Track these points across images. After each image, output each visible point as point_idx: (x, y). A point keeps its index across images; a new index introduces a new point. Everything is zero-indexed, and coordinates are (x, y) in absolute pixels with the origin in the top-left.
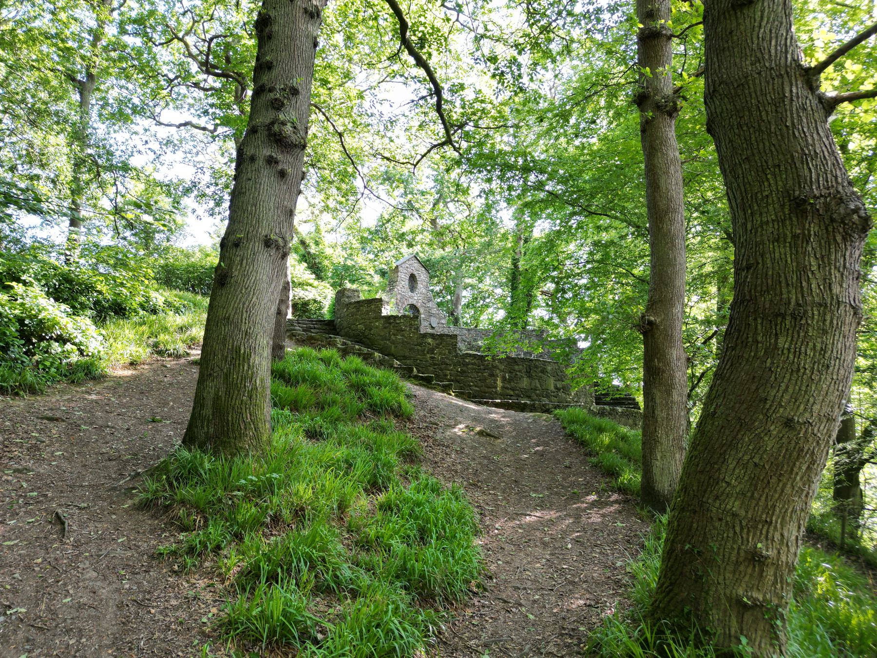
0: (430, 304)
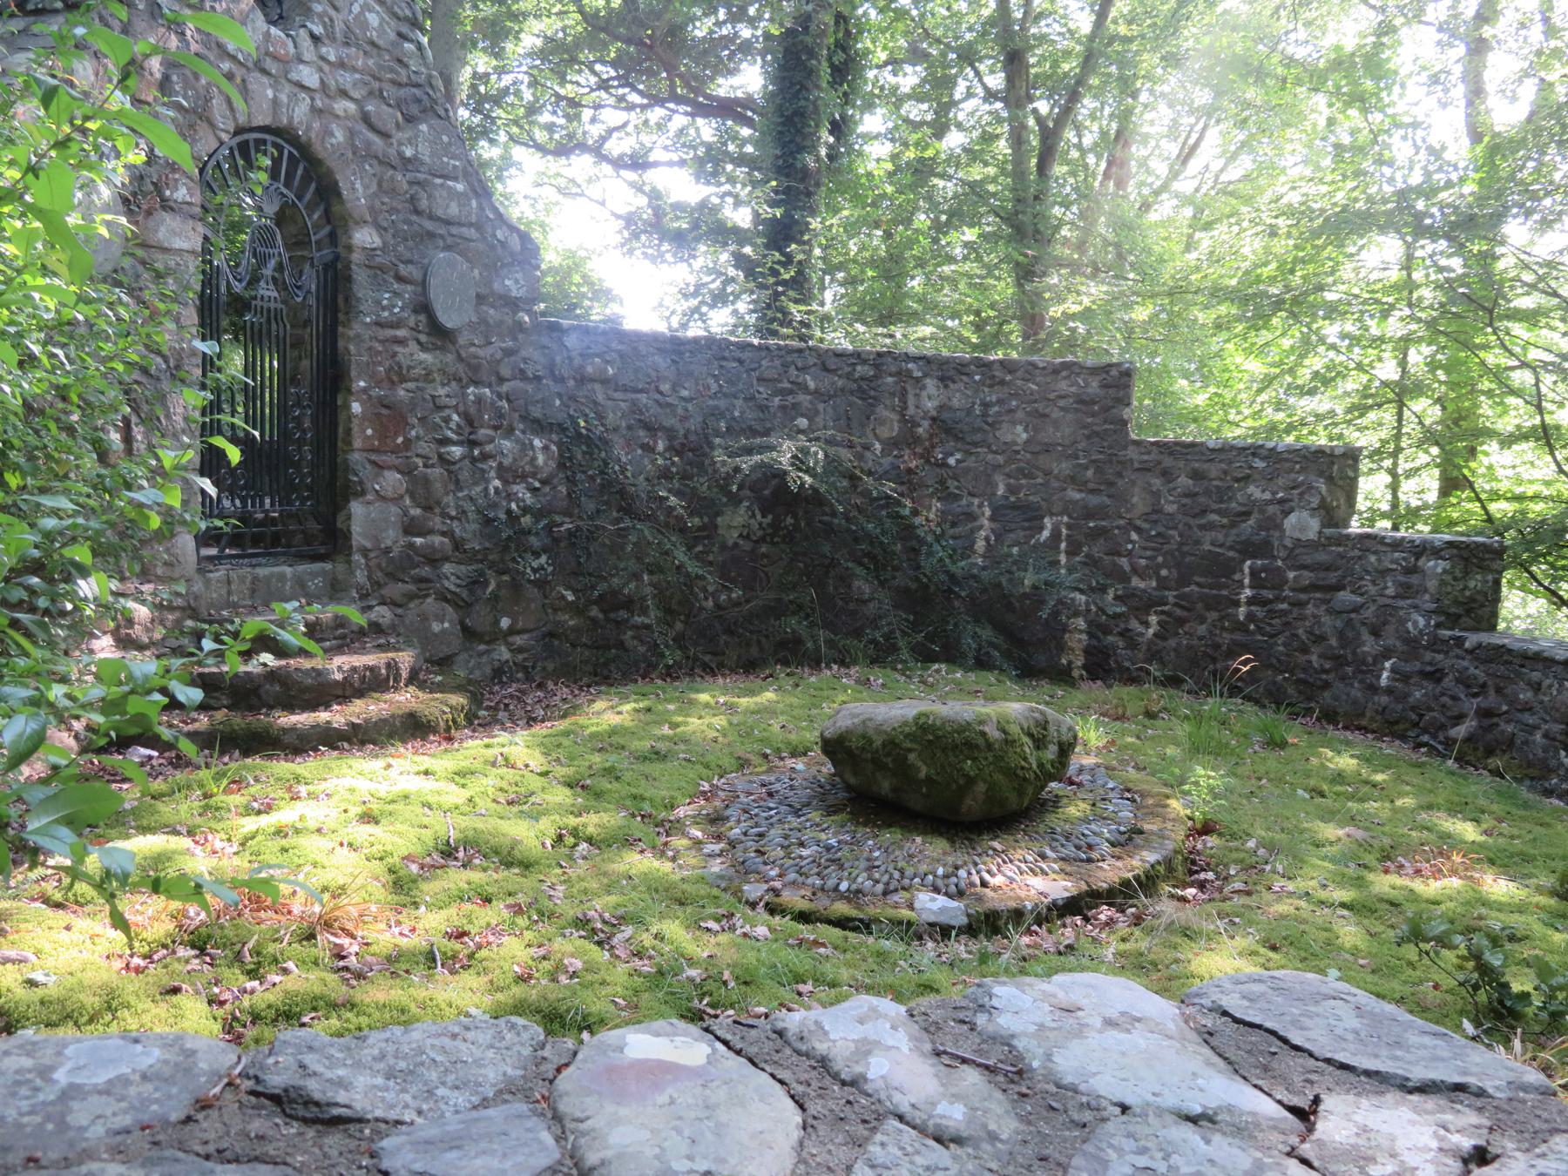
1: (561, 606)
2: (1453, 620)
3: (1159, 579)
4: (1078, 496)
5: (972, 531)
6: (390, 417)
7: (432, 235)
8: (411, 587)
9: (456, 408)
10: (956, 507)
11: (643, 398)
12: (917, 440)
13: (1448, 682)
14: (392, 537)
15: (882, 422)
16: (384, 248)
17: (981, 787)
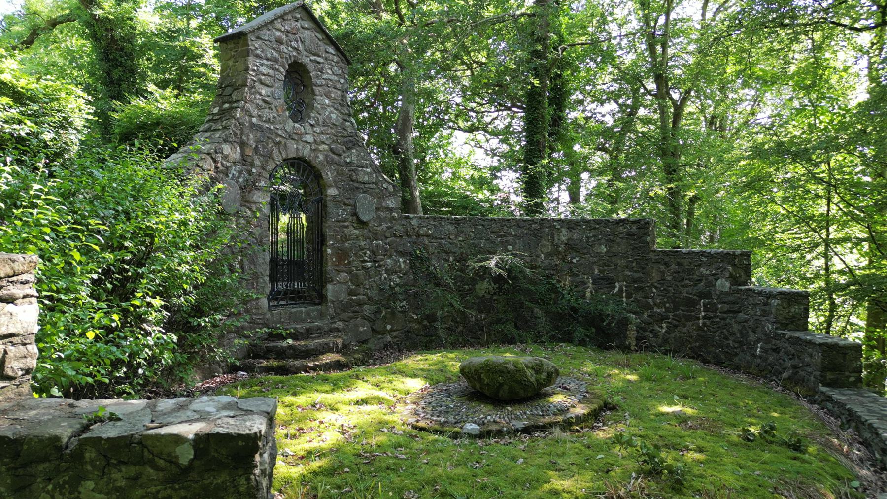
0: (353, 157)
1: (412, 320)
2: (785, 326)
3: (666, 308)
6: (342, 254)
7: (358, 188)
9: (368, 249)
10: (577, 279)
11: (443, 241)
12: (559, 253)
13: (781, 353)
14: (343, 297)
15: (544, 246)
16: (339, 195)
17: (506, 387)
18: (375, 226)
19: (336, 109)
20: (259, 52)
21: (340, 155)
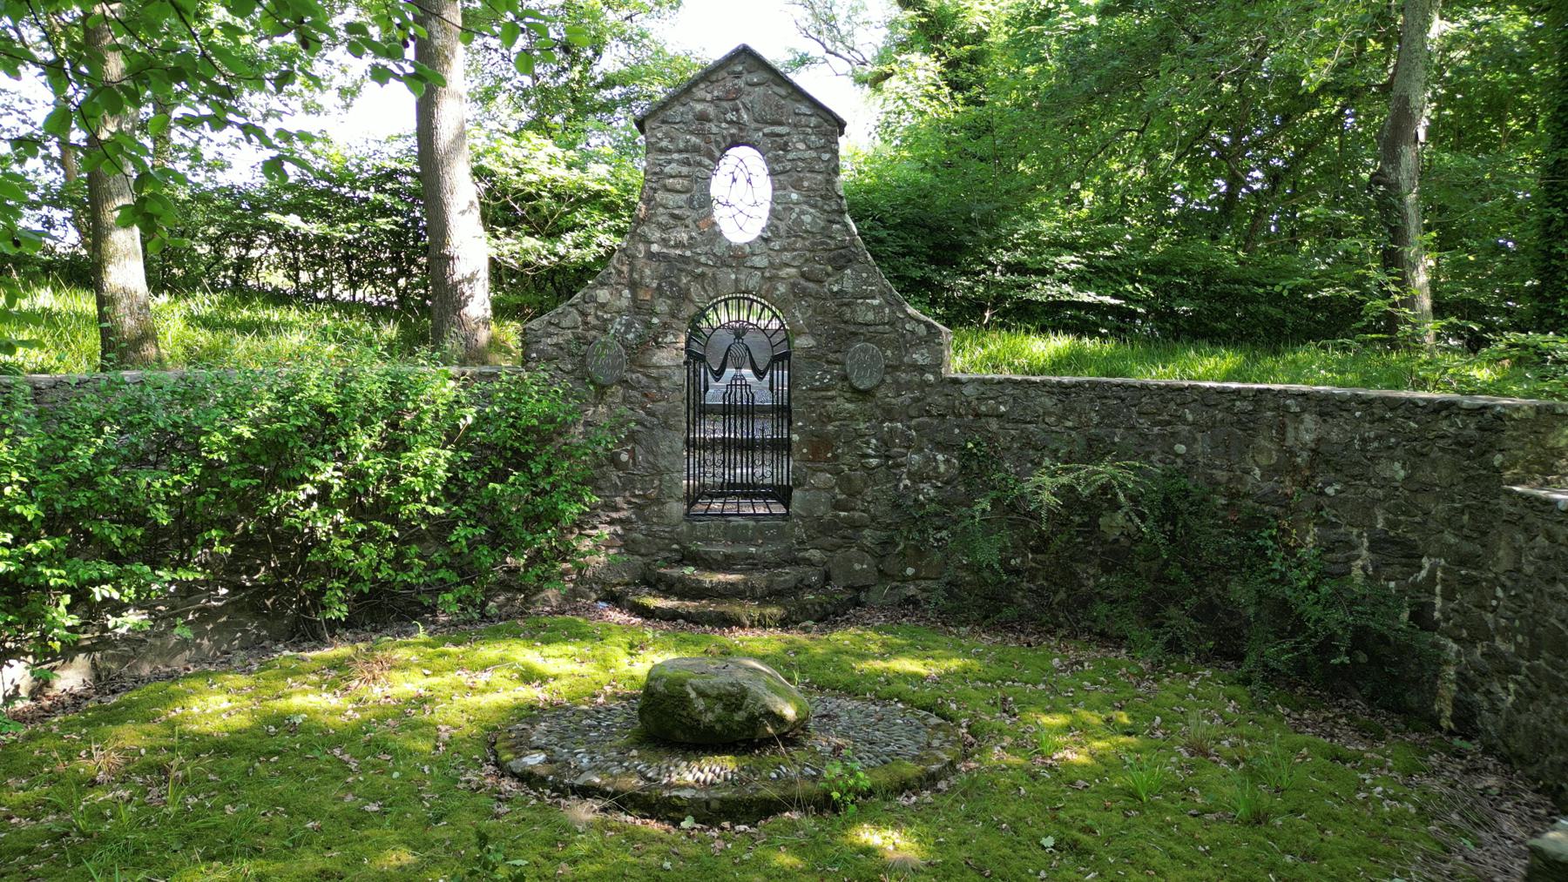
3: (1517, 644)
4: (1453, 540)
5: (1349, 560)
7: (854, 334)
8: (840, 541)
9: (874, 436)
10: (1332, 535)
11: (1031, 427)
12: (1296, 469)
15: (1260, 451)
18: (886, 395)
19: (814, 206)
20: (664, 144)
21: (820, 282)
